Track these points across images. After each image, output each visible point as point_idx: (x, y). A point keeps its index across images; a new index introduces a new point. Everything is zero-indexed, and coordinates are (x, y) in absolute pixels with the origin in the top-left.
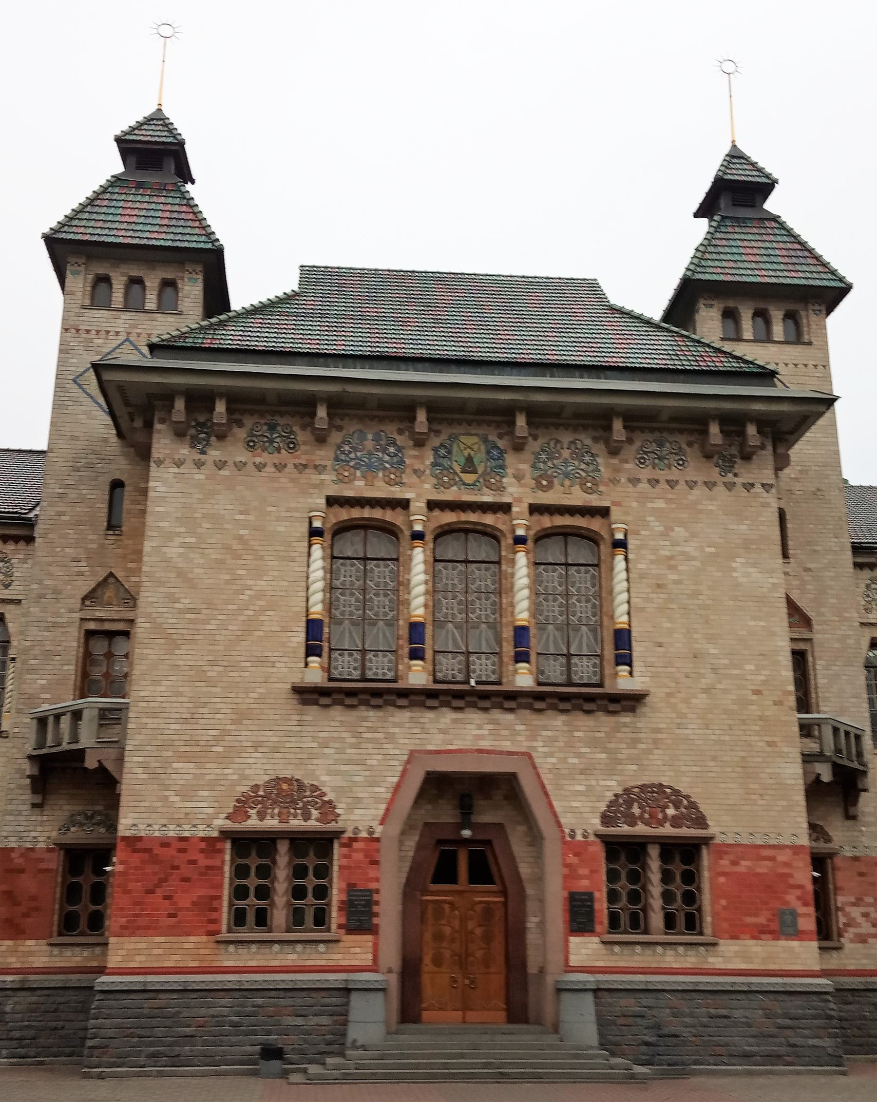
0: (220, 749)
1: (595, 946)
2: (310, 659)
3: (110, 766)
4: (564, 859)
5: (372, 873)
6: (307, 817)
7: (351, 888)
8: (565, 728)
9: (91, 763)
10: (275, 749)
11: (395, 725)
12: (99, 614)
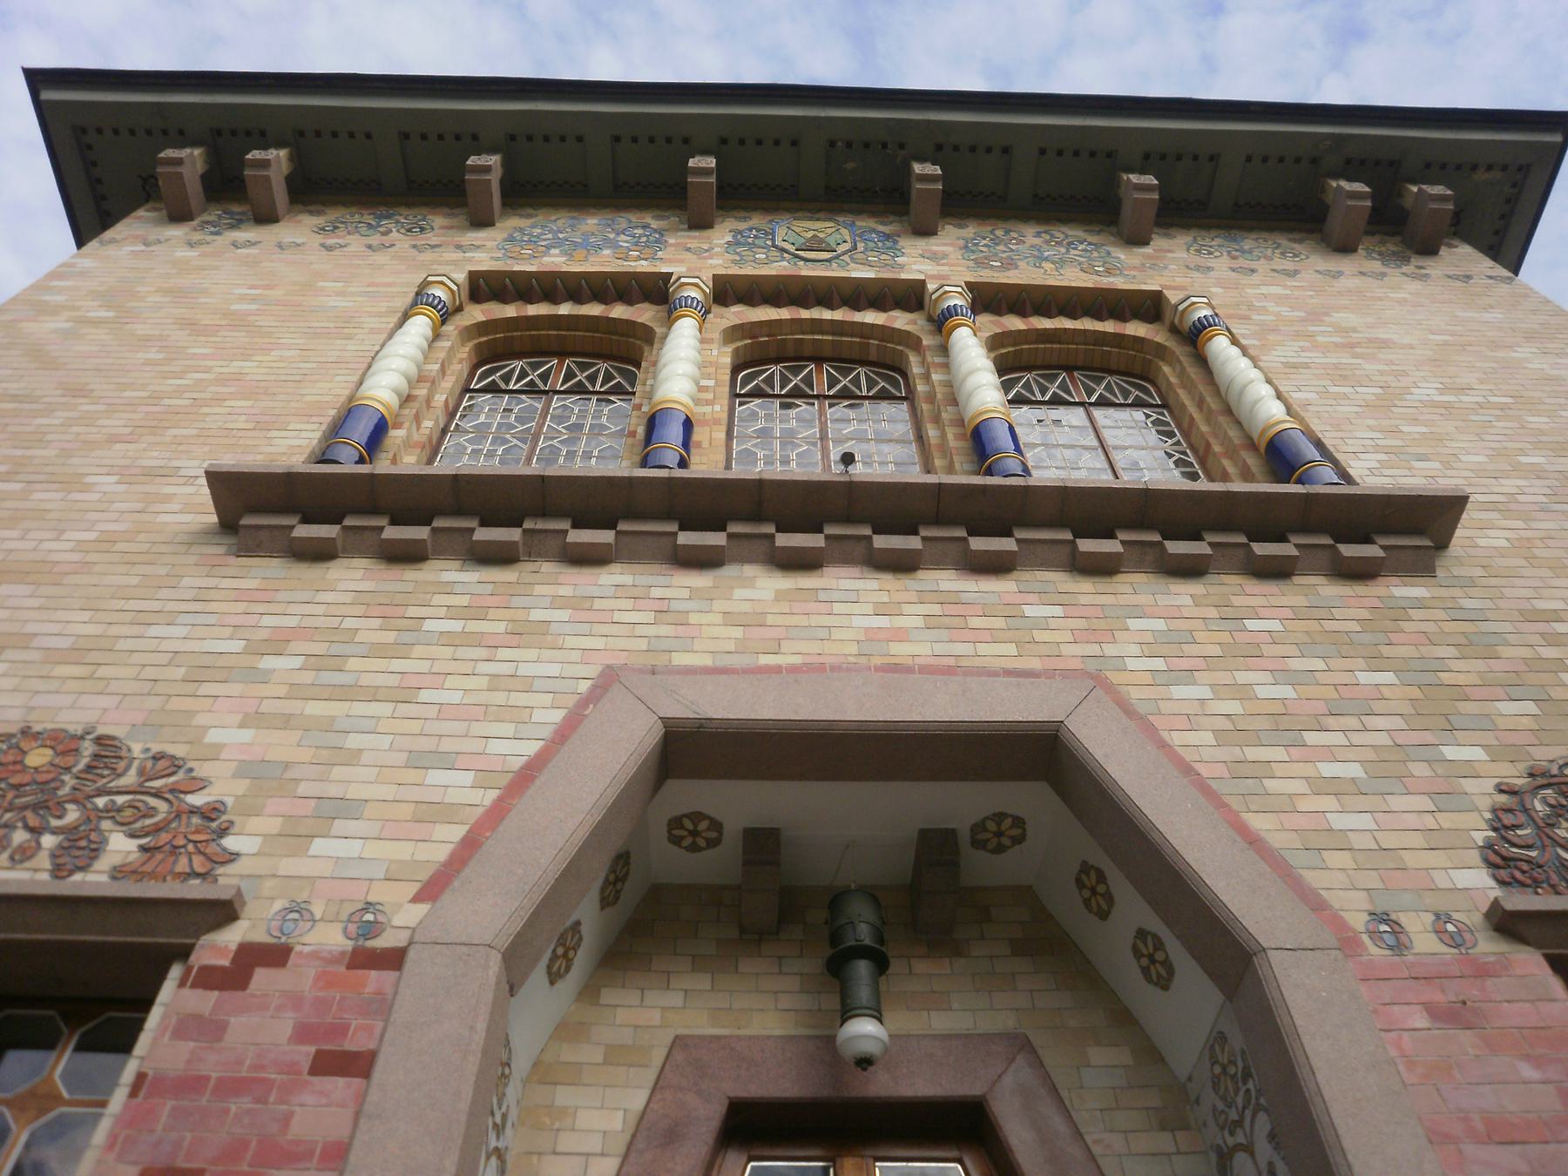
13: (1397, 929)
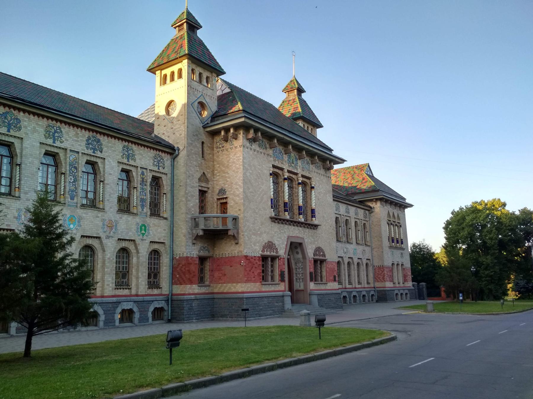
3: (236, 235)
12: (203, 185)
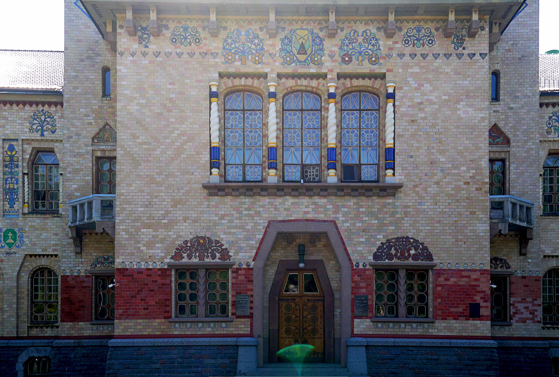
0: (166, 221)
1: (368, 324)
2: (213, 170)
3: (108, 230)
4: (352, 279)
5: (249, 287)
6: (214, 257)
7: (238, 293)
8: (355, 207)
9: (99, 230)
10: (195, 221)
11: (260, 206)
13: (359, 264)
